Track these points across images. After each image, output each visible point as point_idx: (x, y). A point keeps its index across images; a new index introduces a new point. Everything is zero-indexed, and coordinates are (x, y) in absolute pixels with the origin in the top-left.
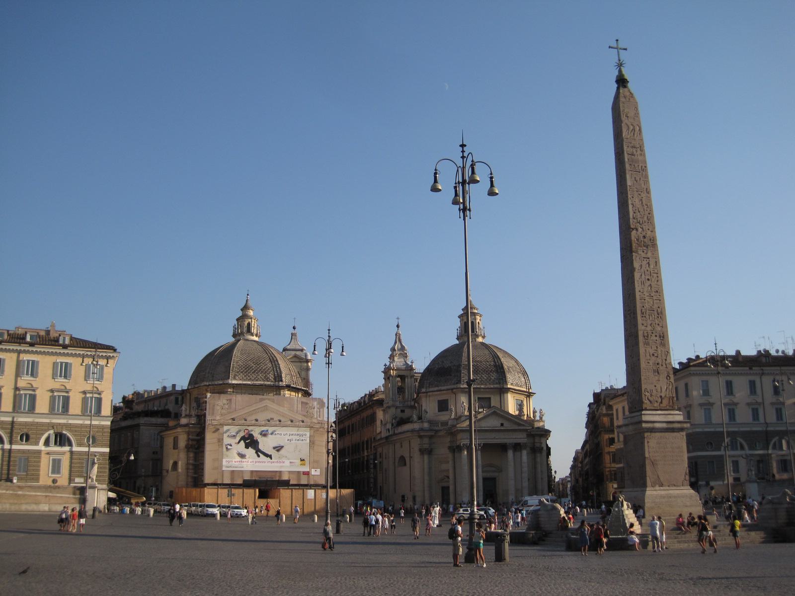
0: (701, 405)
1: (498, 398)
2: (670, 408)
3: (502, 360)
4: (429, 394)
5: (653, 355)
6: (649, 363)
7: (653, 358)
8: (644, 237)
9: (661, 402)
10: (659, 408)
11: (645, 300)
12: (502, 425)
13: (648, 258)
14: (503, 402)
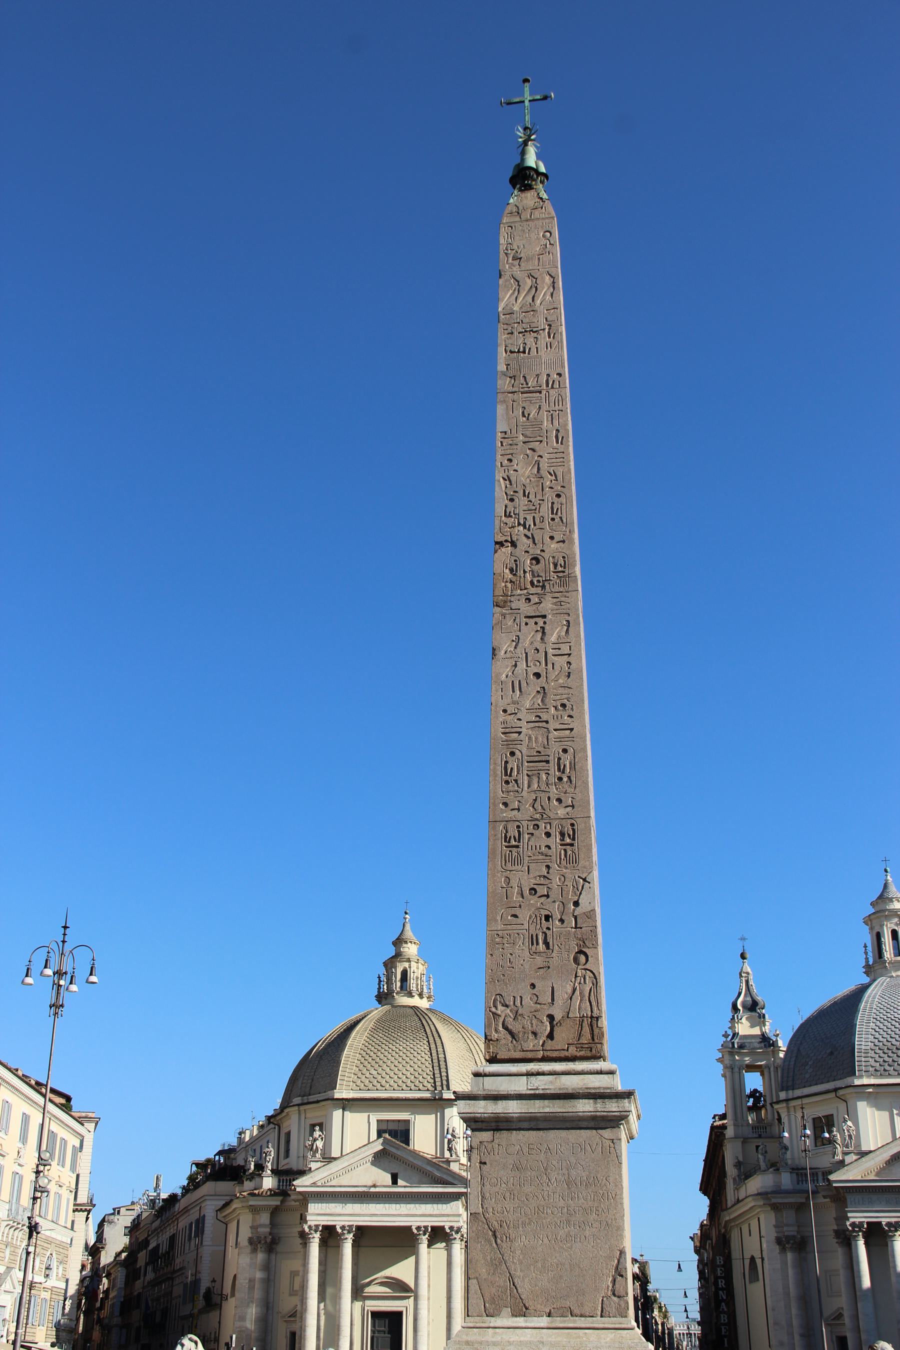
2: (582, 1053)
4: (792, 1103)
5: (533, 891)
6: (515, 916)
7: (533, 900)
8: (536, 560)
9: (551, 1036)
10: (540, 1055)
11: (520, 733)
13: (544, 617)
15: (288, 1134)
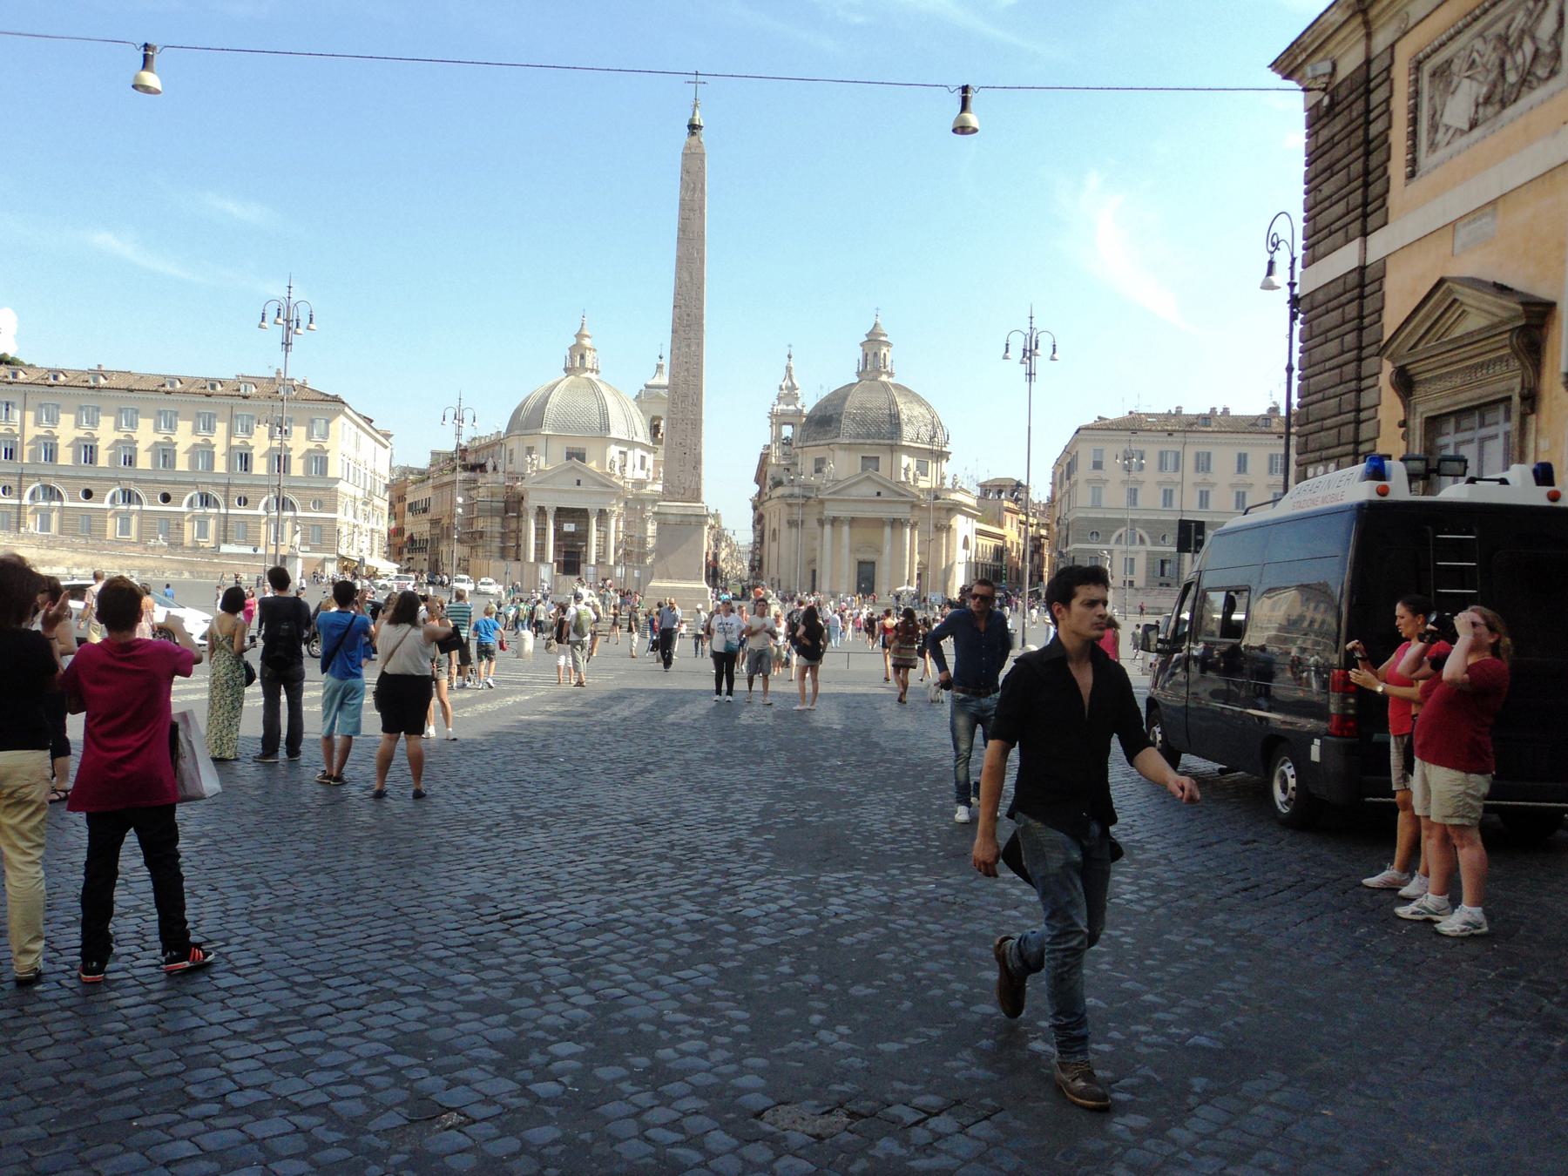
0: (1088, 481)
1: (889, 456)
3: (901, 406)
12: (879, 494)
14: (894, 467)
15: (511, 450)
